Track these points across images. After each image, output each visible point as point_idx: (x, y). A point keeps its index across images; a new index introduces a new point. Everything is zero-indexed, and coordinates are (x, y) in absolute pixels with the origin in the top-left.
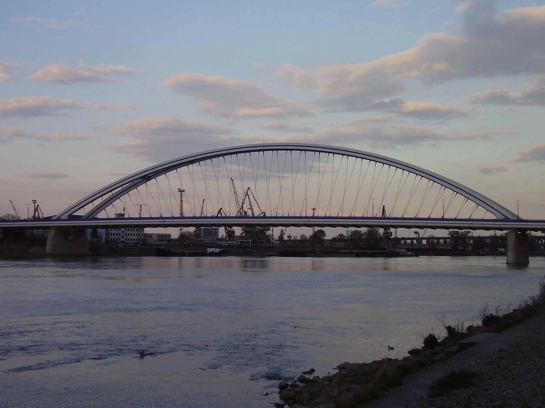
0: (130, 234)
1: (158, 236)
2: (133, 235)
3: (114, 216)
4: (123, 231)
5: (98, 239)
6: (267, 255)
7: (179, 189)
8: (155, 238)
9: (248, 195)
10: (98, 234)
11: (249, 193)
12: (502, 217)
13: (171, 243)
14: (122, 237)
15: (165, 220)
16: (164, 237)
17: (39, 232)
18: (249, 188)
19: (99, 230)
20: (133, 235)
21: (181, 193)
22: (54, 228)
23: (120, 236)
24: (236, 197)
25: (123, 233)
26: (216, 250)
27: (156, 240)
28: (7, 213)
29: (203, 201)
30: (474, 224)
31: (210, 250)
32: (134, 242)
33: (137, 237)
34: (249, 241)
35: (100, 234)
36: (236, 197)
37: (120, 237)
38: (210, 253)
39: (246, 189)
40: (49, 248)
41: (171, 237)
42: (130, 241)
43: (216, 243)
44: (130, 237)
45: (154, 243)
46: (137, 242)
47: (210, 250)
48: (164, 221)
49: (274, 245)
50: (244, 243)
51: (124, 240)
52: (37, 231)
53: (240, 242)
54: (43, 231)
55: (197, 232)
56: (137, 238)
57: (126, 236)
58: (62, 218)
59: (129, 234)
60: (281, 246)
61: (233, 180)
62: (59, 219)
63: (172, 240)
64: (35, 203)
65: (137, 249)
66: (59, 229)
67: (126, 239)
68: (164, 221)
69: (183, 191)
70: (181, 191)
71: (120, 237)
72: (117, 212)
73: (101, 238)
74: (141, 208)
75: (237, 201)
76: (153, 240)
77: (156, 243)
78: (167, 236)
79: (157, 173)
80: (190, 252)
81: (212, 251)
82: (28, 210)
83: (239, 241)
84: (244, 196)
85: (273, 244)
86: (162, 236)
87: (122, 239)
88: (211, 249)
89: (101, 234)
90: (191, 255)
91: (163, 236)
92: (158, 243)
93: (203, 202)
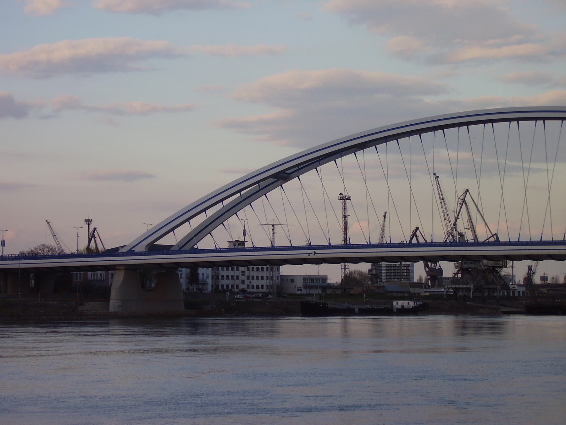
0: (255, 278)
1: (304, 279)
2: (260, 278)
3: (226, 246)
4: (243, 272)
5: (200, 287)
6: (502, 312)
7: (340, 194)
8: (299, 283)
9: (466, 204)
11: (468, 199)
13: (328, 291)
14: (241, 282)
15: (317, 251)
17: (97, 276)
18: (467, 191)
19: (201, 271)
20: (260, 278)
21: (345, 202)
22: (123, 268)
23: (237, 281)
24: (444, 207)
25: (242, 275)
26: (409, 303)
28: (42, 244)
29: (385, 216)
31: (398, 304)
33: (268, 281)
34: (468, 286)
35: (203, 277)
36: (444, 207)
37: (238, 282)
38: (398, 309)
39: (461, 192)
40: (114, 304)
41: (329, 281)
42: (255, 290)
43: (409, 292)
44: (255, 282)
45: (298, 293)
46: (268, 291)
47: (398, 304)
48: (314, 251)
49: (516, 295)
50: (460, 291)
51: (244, 287)
52: (94, 274)
53: (453, 288)
54: (104, 274)
55: (374, 272)
56: (268, 284)
57: (248, 281)
58: (137, 249)
59: (253, 277)
60: (529, 295)
61: (438, 177)
62: (131, 252)
63: (330, 287)
64: (89, 224)
65: (267, 303)
66: (130, 269)
67: (248, 286)
68: (315, 253)
69: (347, 199)
70: (344, 198)
71: (238, 282)
73: (205, 284)
74: (273, 229)
75: (446, 215)
76: (296, 287)
77: (301, 292)
79: (300, 167)
80: (362, 307)
81: (403, 306)
82: (78, 237)
83: (450, 286)
84: (459, 206)
85: (514, 293)
86: (311, 279)
87: (242, 287)
88: (401, 303)
89: (205, 277)
90: (364, 312)
91: (314, 279)
92: (304, 291)
93: (385, 218)
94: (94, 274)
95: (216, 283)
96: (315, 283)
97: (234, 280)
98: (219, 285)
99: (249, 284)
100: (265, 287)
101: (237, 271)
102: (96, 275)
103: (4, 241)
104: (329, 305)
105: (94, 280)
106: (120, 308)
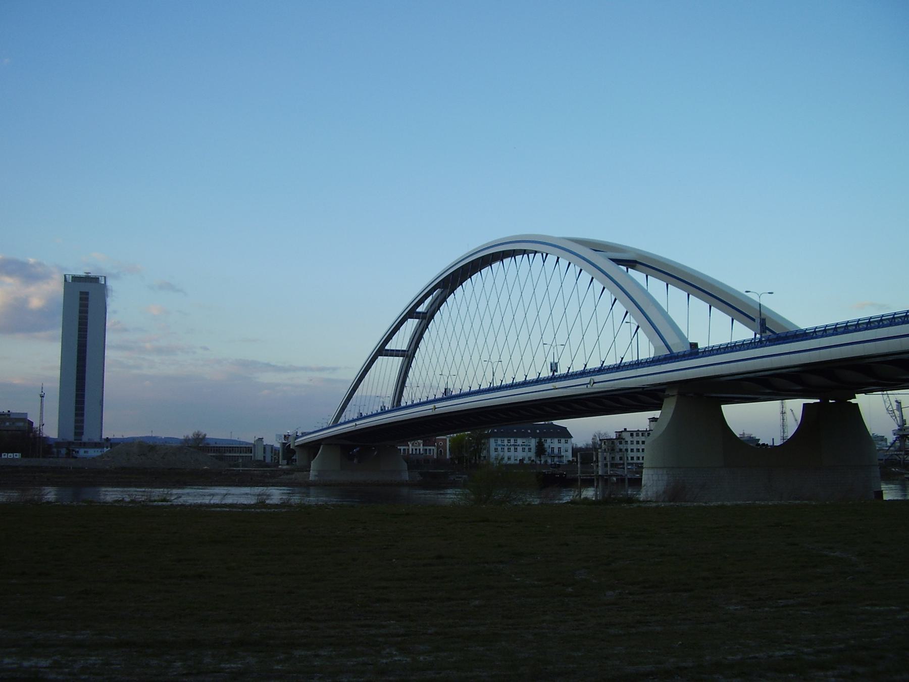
10: (556, 451)
40: (312, 475)
52: (416, 449)
54: (433, 450)
68: (356, 425)
73: (561, 457)
89: (562, 451)
94: (416, 449)
105: (416, 454)
106: (317, 478)
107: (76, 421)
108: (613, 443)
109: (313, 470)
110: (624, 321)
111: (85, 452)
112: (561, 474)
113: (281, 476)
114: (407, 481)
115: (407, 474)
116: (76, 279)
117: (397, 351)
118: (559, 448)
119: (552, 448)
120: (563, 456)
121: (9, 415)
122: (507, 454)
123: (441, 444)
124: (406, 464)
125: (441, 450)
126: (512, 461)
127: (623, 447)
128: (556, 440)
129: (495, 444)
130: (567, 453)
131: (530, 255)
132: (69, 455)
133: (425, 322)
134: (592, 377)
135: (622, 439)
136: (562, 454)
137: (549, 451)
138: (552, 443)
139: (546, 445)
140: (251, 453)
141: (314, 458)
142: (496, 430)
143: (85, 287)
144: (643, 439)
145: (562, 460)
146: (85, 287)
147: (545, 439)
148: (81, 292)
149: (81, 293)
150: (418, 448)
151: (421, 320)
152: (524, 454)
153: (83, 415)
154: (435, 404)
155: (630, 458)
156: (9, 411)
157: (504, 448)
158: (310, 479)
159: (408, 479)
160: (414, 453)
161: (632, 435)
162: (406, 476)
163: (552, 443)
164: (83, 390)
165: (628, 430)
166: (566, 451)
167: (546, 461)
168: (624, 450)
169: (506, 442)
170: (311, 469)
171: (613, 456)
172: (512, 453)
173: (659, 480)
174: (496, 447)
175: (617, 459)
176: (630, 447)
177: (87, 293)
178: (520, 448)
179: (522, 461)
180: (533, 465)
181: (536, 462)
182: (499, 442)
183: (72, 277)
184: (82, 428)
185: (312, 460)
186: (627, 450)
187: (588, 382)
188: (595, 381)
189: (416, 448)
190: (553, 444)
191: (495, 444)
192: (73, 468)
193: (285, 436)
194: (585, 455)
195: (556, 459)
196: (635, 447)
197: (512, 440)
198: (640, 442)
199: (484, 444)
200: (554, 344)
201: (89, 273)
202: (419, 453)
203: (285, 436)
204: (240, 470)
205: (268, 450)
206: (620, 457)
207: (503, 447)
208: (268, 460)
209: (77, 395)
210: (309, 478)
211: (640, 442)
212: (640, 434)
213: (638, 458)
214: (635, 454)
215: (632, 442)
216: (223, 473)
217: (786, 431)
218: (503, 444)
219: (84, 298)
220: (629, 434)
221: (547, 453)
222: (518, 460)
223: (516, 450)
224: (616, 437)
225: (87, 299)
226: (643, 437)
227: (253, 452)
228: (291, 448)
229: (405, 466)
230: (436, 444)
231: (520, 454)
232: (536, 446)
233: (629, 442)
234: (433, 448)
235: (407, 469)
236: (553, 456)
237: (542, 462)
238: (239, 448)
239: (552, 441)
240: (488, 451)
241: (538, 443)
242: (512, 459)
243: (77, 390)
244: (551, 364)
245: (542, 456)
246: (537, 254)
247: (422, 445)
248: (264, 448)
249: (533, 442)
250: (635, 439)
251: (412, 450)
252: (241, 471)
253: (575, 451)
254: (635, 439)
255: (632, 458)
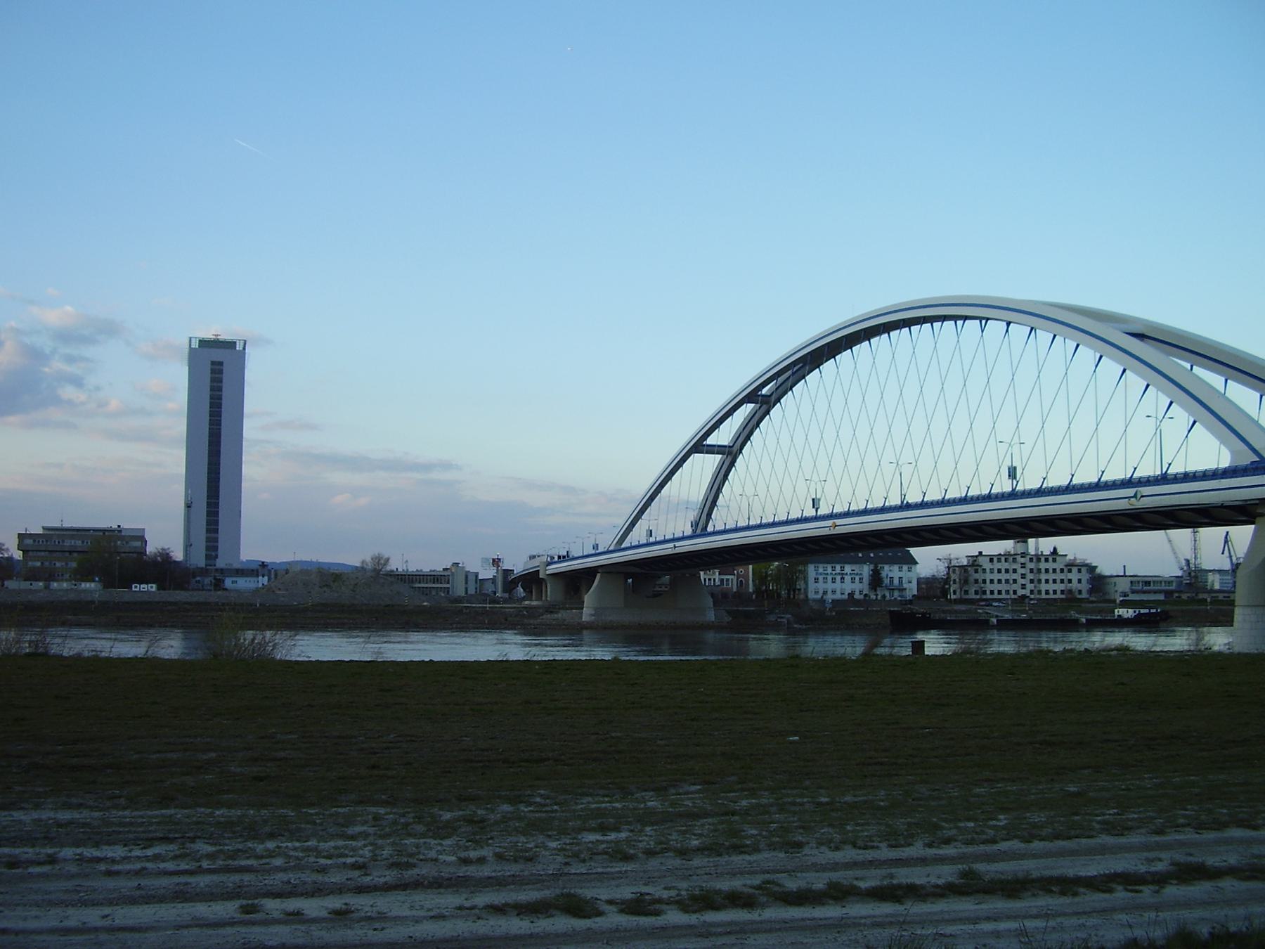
4: (1022, 574)
10: (896, 582)
12: (1248, 458)
14: (1020, 586)
15: (677, 544)
16: (1152, 584)
25: (1022, 578)
26: (1128, 611)
27: (1127, 590)
30: (1139, 496)
32: (1000, 597)
37: (1015, 587)
40: (587, 614)
46: (1063, 596)
52: (710, 579)
54: (732, 579)
67: (1032, 592)
68: (675, 547)
71: (1015, 587)
72: (1166, 534)
73: (902, 590)
76: (1118, 592)
78: (1163, 583)
80: (1089, 617)
87: (1021, 592)
94: (710, 579)
95: (983, 587)
96: (1152, 587)
97: (1008, 585)
98: (986, 591)
99: (1033, 588)
100: (1059, 592)
101: (1069, 574)
102: (712, 580)
103: (597, 545)
104: (932, 616)
106: (593, 617)
107: (208, 540)
108: (966, 571)
109: (587, 607)
110: (1167, 415)
111: (233, 582)
112: (924, 614)
113: (542, 615)
114: (713, 622)
115: (713, 612)
116: (204, 343)
117: (719, 446)
118: (900, 578)
119: (890, 578)
120: (905, 589)
121: (120, 531)
122: (830, 586)
123: (741, 572)
124: (712, 600)
125: (741, 581)
126: (838, 596)
127: (980, 576)
128: (896, 568)
129: (815, 572)
130: (910, 584)
131: (958, 322)
132: (218, 585)
133: (765, 407)
134: (1140, 489)
135: (978, 565)
136: (905, 586)
137: (887, 581)
138: (890, 570)
139: (884, 574)
140: (448, 583)
141: (587, 592)
142: (860, 555)
143: (218, 355)
144: (1006, 565)
145: (904, 593)
146: (218, 355)
147: (882, 565)
148: (212, 362)
149: (213, 363)
150: (712, 578)
151: (759, 405)
152: (853, 586)
153: (216, 531)
154: (835, 521)
155: (988, 592)
156: (119, 526)
157: (826, 578)
158: (583, 620)
159: (713, 619)
160: (707, 584)
161: (991, 560)
162: (711, 616)
163: (890, 570)
164: (218, 497)
165: (984, 554)
166: (910, 582)
167: (884, 596)
168: (980, 581)
169: (829, 570)
170: (585, 606)
171: (967, 589)
172: (838, 585)
173: (1258, 622)
174: (817, 577)
175: (972, 593)
176: (988, 577)
177: (221, 364)
178: (848, 579)
179: (851, 595)
180: (866, 601)
181: (870, 597)
182: (821, 570)
183: (200, 341)
184: (216, 549)
185: (586, 594)
186: (984, 581)
187: (1132, 495)
188: (1144, 494)
189: (709, 577)
190: (892, 572)
191: (815, 572)
192: (260, 605)
193: (494, 560)
194: (933, 588)
195: (896, 594)
196: (996, 577)
197: (838, 567)
198: (1003, 571)
199: (800, 571)
200: (1016, 440)
201: (218, 335)
202: (714, 584)
203: (494, 560)
204: (486, 607)
205: (471, 579)
206: (975, 591)
207: (825, 576)
208: (472, 591)
209: (209, 505)
210: (582, 619)
211: (1003, 571)
212: (1003, 559)
213: (1000, 592)
214: (996, 587)
215: (992, 571)
216: (464, 611)
217: (1199, 556)
218: (825, 572)
219: (217, 370)
220: (988, 558)
221: (884, 585)
222: (847, 594)
223: (843, 578)
224: (968, 563)
225: (221, 372)
226: (1007, 564)
227: (450, 582)
228: (540, 577)
229: (710, 601)
230: (735, 572)
231: (848, 587)
232: (869, 576)
233: (988, 571)
234: (732, 577)
235: (712, 606)
236: (893, 589)
237: (879, 597)
238: (447, 578)
239: (891, 568)
240: (806, 583)
241: (872, 570)
242: (838, 592)
243: (208, 497)
244: (1009, 469)
245: (878, 589)
246: (989, 321)
247: (717, 573)
248: (467, 577)
249: (866, 570)
250: (997, 566)
251: (705, 579)
252: (488, 609)
253: (919, 581)
254: (997, 566)
255: (992, 592)
